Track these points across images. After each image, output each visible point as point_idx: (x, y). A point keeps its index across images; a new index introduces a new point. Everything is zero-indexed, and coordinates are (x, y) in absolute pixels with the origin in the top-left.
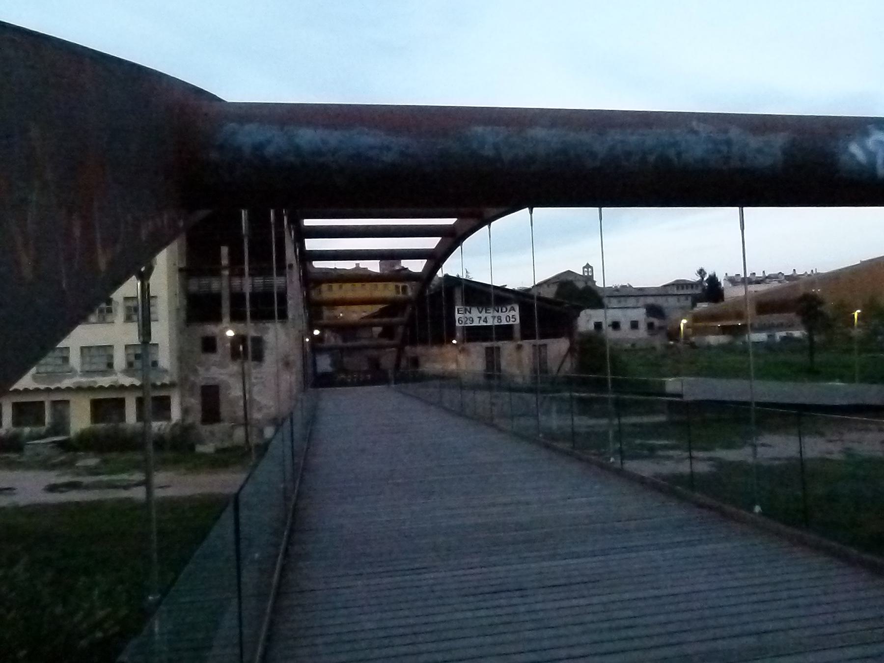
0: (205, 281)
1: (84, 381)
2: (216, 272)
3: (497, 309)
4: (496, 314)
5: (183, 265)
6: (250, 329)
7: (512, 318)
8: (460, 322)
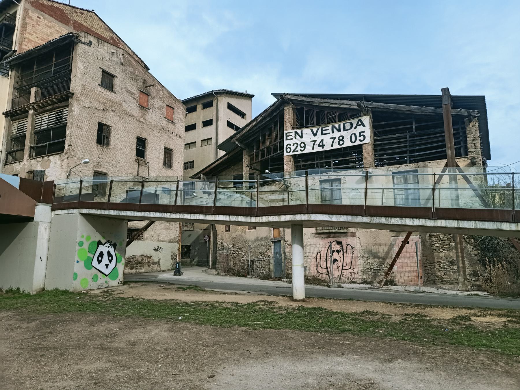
3: (337, 126)
4: (337, 134)
7: (360, 136)
8: (289, 150)
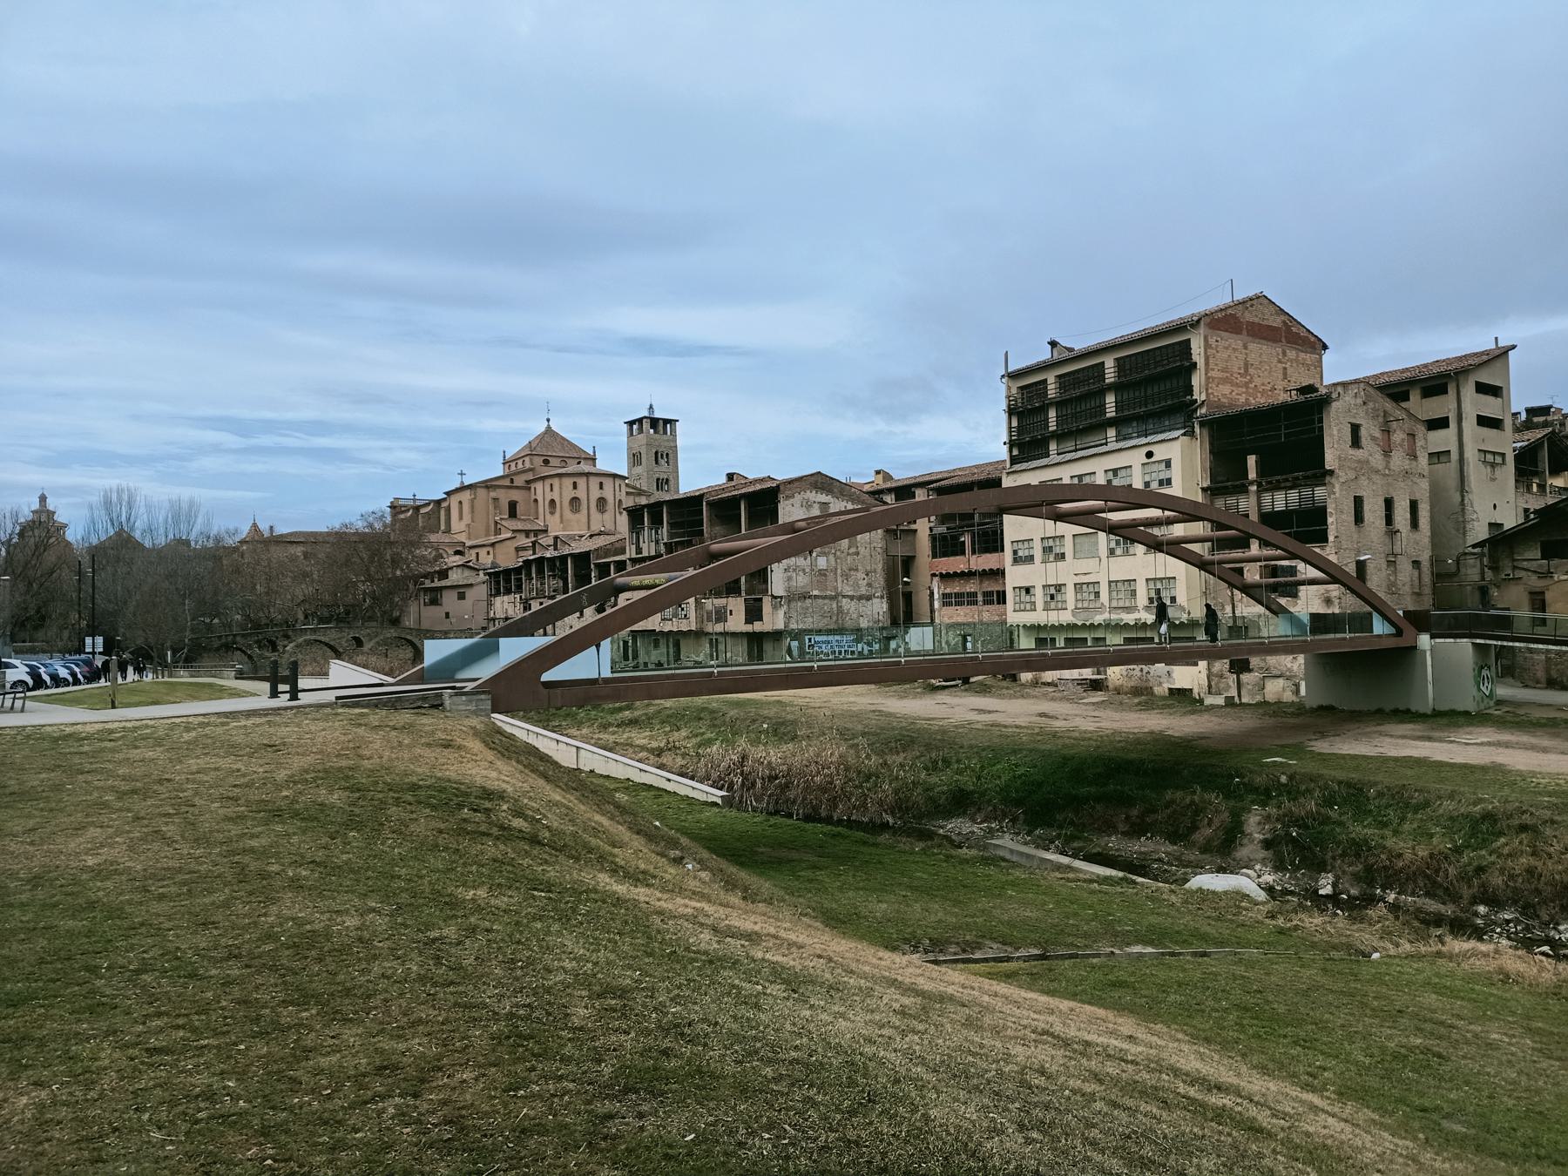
0: (1231, 500)
2: (1243, 490)
5: (1207, 483)
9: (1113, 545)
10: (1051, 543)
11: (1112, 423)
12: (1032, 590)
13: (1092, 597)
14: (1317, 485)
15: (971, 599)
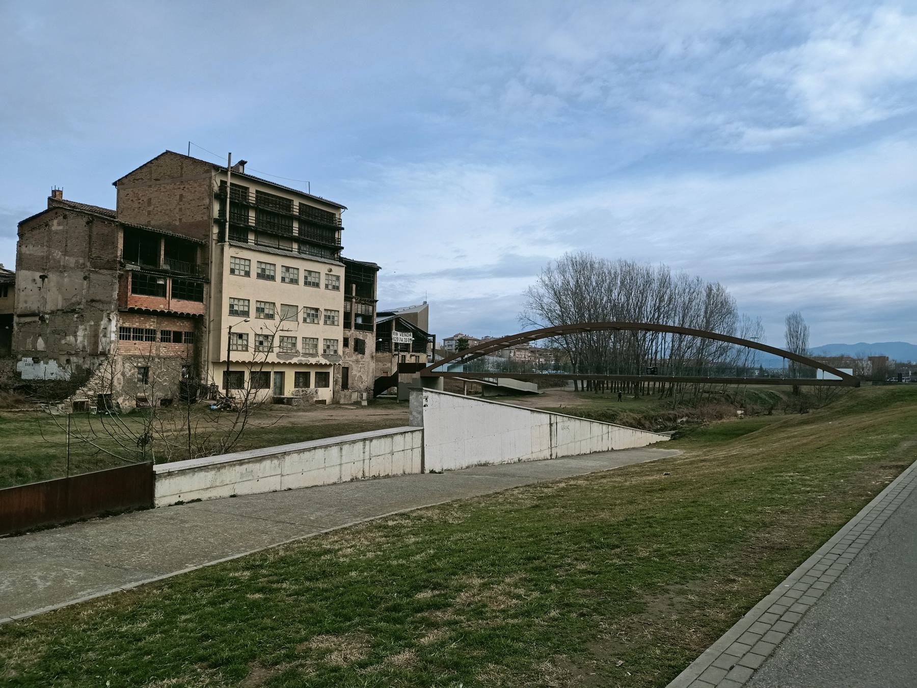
1: (304, 360)
6: (360, 335)
9: (305, 316)
10: (262, 305)
11: (295, 240)
12: (245, 337)
13: (290, 346)
14: (370, 305)
15: (150, 336)
